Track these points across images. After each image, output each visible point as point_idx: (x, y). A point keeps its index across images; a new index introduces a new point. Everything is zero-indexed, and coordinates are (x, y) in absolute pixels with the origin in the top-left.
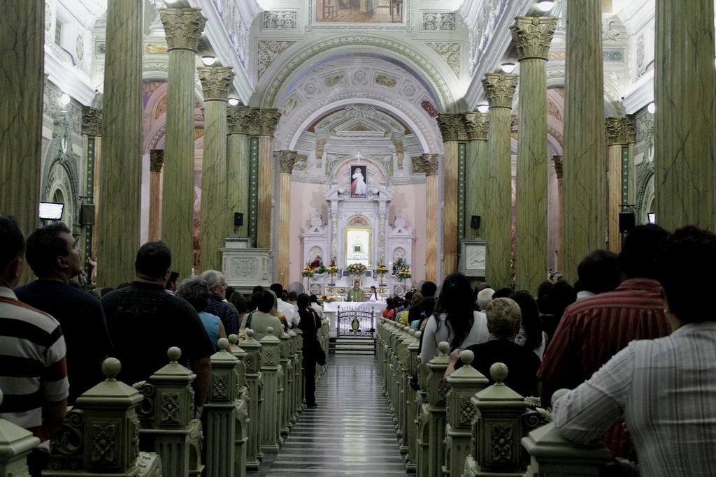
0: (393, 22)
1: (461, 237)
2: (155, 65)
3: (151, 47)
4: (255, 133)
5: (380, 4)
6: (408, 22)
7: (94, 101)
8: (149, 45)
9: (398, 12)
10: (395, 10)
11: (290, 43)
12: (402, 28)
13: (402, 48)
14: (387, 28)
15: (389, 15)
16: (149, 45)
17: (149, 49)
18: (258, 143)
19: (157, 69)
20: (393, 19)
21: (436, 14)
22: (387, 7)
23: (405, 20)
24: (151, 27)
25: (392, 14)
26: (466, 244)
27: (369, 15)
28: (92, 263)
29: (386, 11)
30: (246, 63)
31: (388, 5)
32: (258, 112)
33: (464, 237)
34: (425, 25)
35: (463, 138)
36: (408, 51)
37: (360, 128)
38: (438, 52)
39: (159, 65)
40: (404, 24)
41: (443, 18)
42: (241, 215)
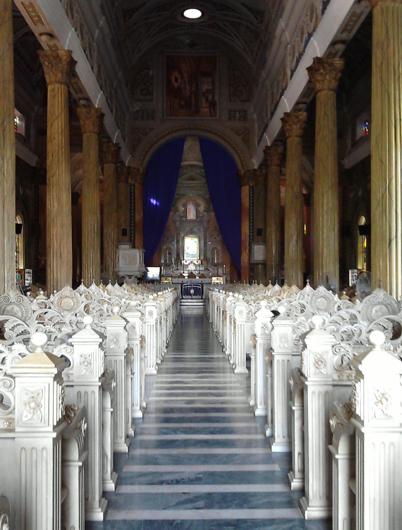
0: (211, 116)
1: (251, 241)
4: (133, 182)
5: (204, 106)
11: (151, 129)
13: (216, 132)
18: (135, 188)
21: (236, 111)
22: (207, 107)
23: (218, 115)
26: (255, 245)
27: (197, 112)
28: (40, 258)
29: (207, 110)
30: (126, 141)
31: (208, 106)
32: (134, 170)
33: (253, 240)
34: (230, 119)
35: (251, 184)
37: (192, 179)
38: (237, 134)
40: (217, 118)
41: (239, 114)
42: (126, 230)
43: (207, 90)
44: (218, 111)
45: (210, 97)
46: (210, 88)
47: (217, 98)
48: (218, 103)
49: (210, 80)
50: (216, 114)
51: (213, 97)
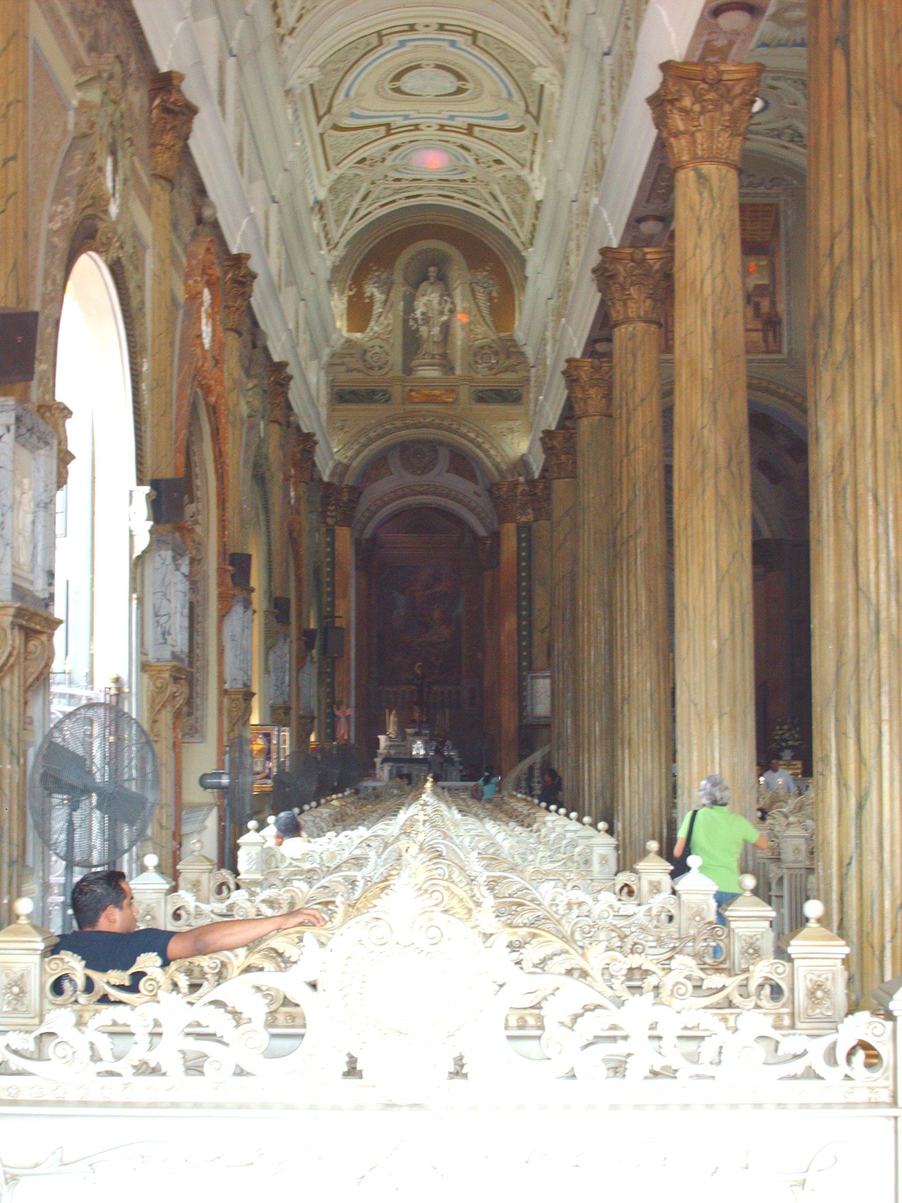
0: (768, 352)
2: (422, 420)
3: (414, 394)
6: (790, 352)
7: (332, 474)
8: (411, 390)
9: (775, 338)
10: (770, 335)
12: (782, 361)
14: (760, 361)
15: (761, 343)
16: (411, 390)
17: (411, 396)
19: (424, 426)
20: (767, 346)
22: (757, 330)
23: (785, 350)
24: (416, 362)
25: (765, 340)
31: (760, 327)
36: (791, 394)
39: (428, 420)
43: (757, 287)
44: (785, 339)
45: (765, 304)
46: (766, 282)
47: (781, 307)
48: (784, 317)
49: (764, 263)
50: (780, 347)
51: (773, 304)
